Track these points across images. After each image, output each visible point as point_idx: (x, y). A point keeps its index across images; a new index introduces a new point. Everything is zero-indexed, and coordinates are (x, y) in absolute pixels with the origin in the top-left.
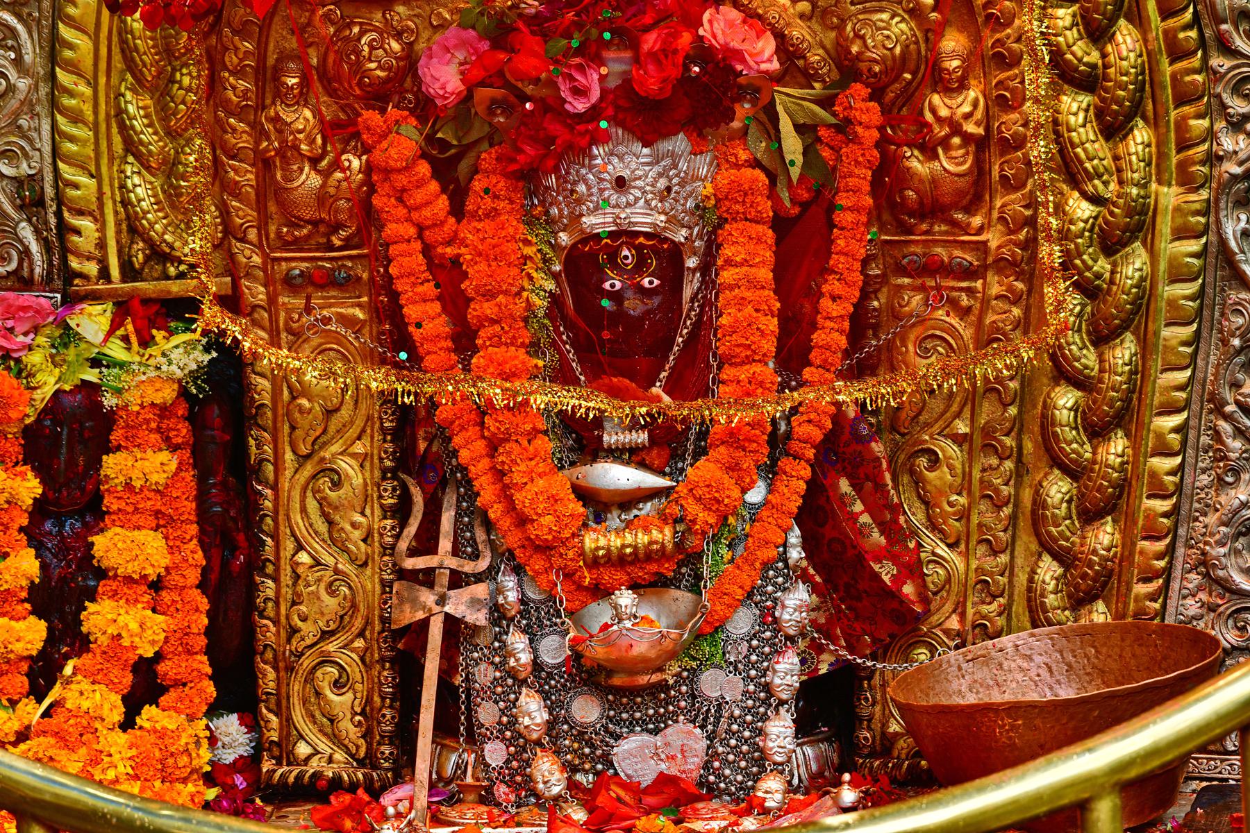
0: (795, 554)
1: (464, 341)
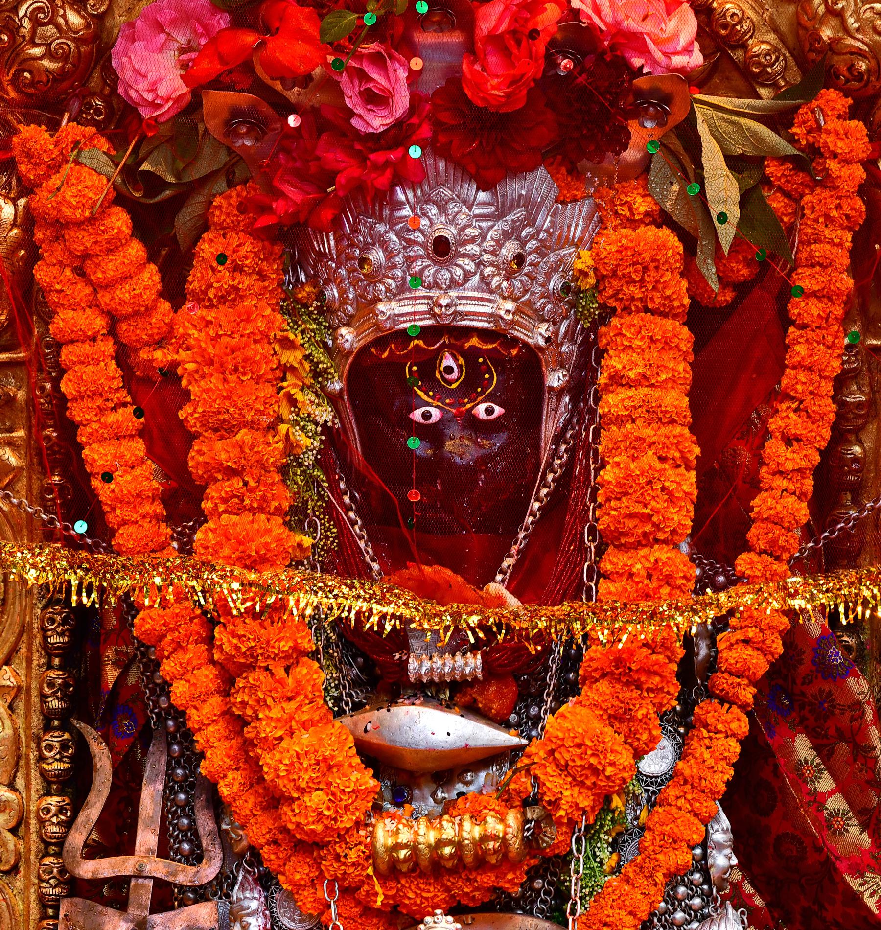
0: (722, 860)
1: (183, 503)
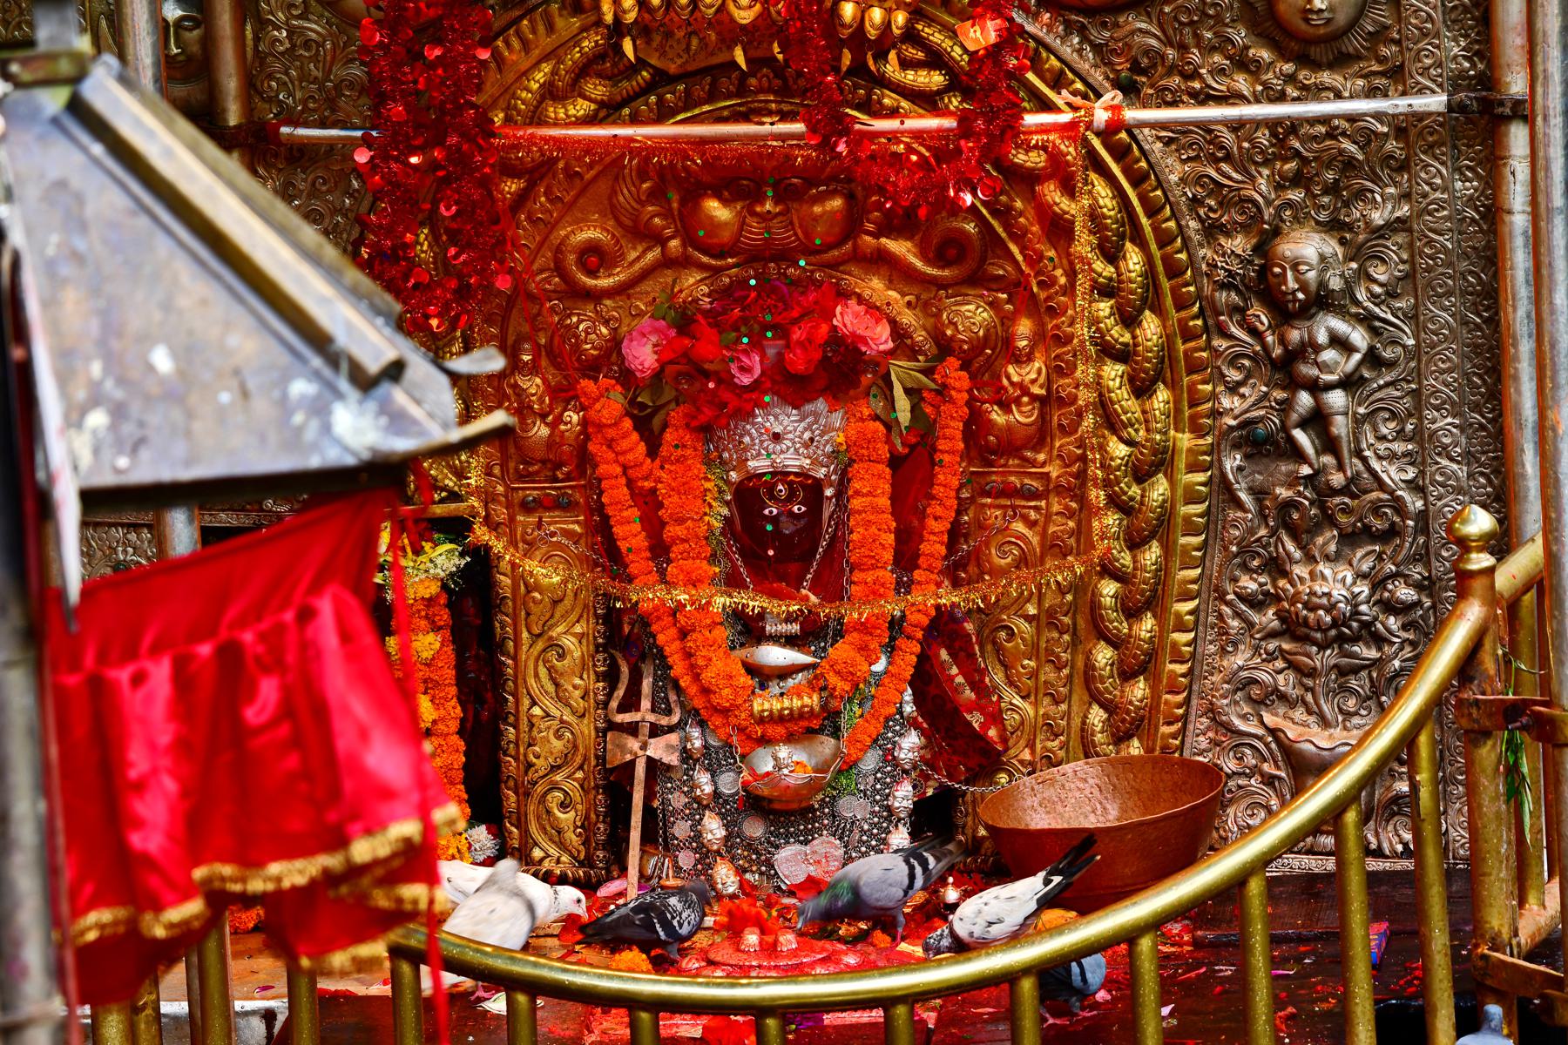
0: (909, 709)
